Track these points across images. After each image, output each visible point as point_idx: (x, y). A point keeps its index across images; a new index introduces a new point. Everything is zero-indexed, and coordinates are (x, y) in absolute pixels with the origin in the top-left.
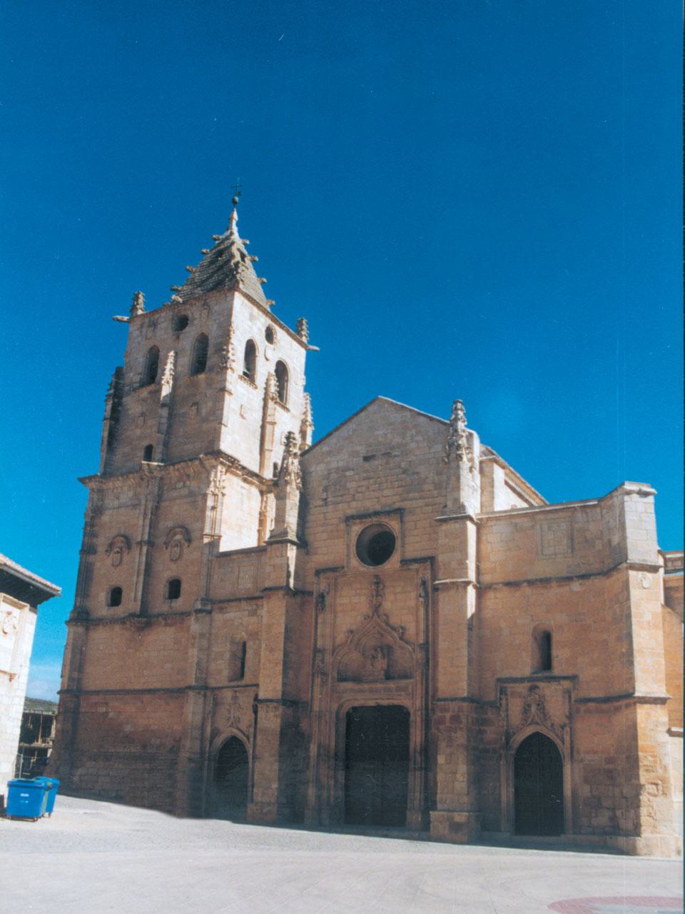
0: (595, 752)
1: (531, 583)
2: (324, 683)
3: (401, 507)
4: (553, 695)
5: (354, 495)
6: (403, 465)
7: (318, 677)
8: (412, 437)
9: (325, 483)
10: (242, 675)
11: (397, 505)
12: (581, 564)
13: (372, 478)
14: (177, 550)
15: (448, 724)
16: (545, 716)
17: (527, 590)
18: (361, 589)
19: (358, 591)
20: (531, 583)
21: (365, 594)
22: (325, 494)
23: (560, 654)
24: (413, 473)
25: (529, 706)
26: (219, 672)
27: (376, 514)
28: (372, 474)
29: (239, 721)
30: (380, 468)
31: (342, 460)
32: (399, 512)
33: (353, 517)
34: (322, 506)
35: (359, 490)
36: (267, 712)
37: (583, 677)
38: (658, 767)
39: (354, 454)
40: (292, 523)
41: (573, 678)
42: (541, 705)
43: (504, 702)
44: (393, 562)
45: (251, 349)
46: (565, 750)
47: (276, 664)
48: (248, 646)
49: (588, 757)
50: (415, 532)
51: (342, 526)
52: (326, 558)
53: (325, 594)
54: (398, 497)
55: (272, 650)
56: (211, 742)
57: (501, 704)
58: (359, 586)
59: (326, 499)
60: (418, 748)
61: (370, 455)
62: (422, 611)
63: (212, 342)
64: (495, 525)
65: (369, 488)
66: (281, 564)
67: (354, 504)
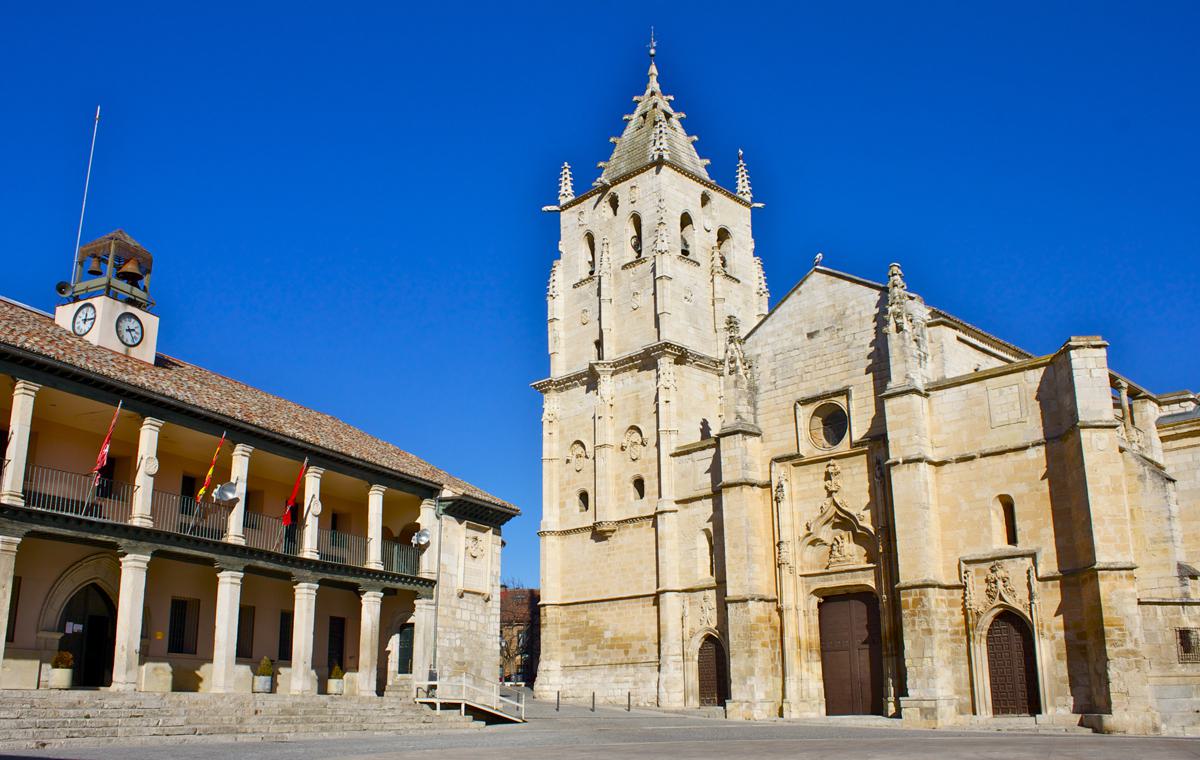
1: (984, 456)
5: (802, 376)
9: (772, 365)
11: (844, 384)
13: (819, 356)
18: (818, 474)
25: (995, 582)
27: (826, 396)
32: (845, 392)
33: (805, 402)
38: (1128, 639)
39: (799, 332)
41: (1033, 556)
52: (781, 444)
53: (783, 483)
54: (845, 374)
58: (816, 471)
60: (888, 635)
61: (813, 331)
67: (803, 385)
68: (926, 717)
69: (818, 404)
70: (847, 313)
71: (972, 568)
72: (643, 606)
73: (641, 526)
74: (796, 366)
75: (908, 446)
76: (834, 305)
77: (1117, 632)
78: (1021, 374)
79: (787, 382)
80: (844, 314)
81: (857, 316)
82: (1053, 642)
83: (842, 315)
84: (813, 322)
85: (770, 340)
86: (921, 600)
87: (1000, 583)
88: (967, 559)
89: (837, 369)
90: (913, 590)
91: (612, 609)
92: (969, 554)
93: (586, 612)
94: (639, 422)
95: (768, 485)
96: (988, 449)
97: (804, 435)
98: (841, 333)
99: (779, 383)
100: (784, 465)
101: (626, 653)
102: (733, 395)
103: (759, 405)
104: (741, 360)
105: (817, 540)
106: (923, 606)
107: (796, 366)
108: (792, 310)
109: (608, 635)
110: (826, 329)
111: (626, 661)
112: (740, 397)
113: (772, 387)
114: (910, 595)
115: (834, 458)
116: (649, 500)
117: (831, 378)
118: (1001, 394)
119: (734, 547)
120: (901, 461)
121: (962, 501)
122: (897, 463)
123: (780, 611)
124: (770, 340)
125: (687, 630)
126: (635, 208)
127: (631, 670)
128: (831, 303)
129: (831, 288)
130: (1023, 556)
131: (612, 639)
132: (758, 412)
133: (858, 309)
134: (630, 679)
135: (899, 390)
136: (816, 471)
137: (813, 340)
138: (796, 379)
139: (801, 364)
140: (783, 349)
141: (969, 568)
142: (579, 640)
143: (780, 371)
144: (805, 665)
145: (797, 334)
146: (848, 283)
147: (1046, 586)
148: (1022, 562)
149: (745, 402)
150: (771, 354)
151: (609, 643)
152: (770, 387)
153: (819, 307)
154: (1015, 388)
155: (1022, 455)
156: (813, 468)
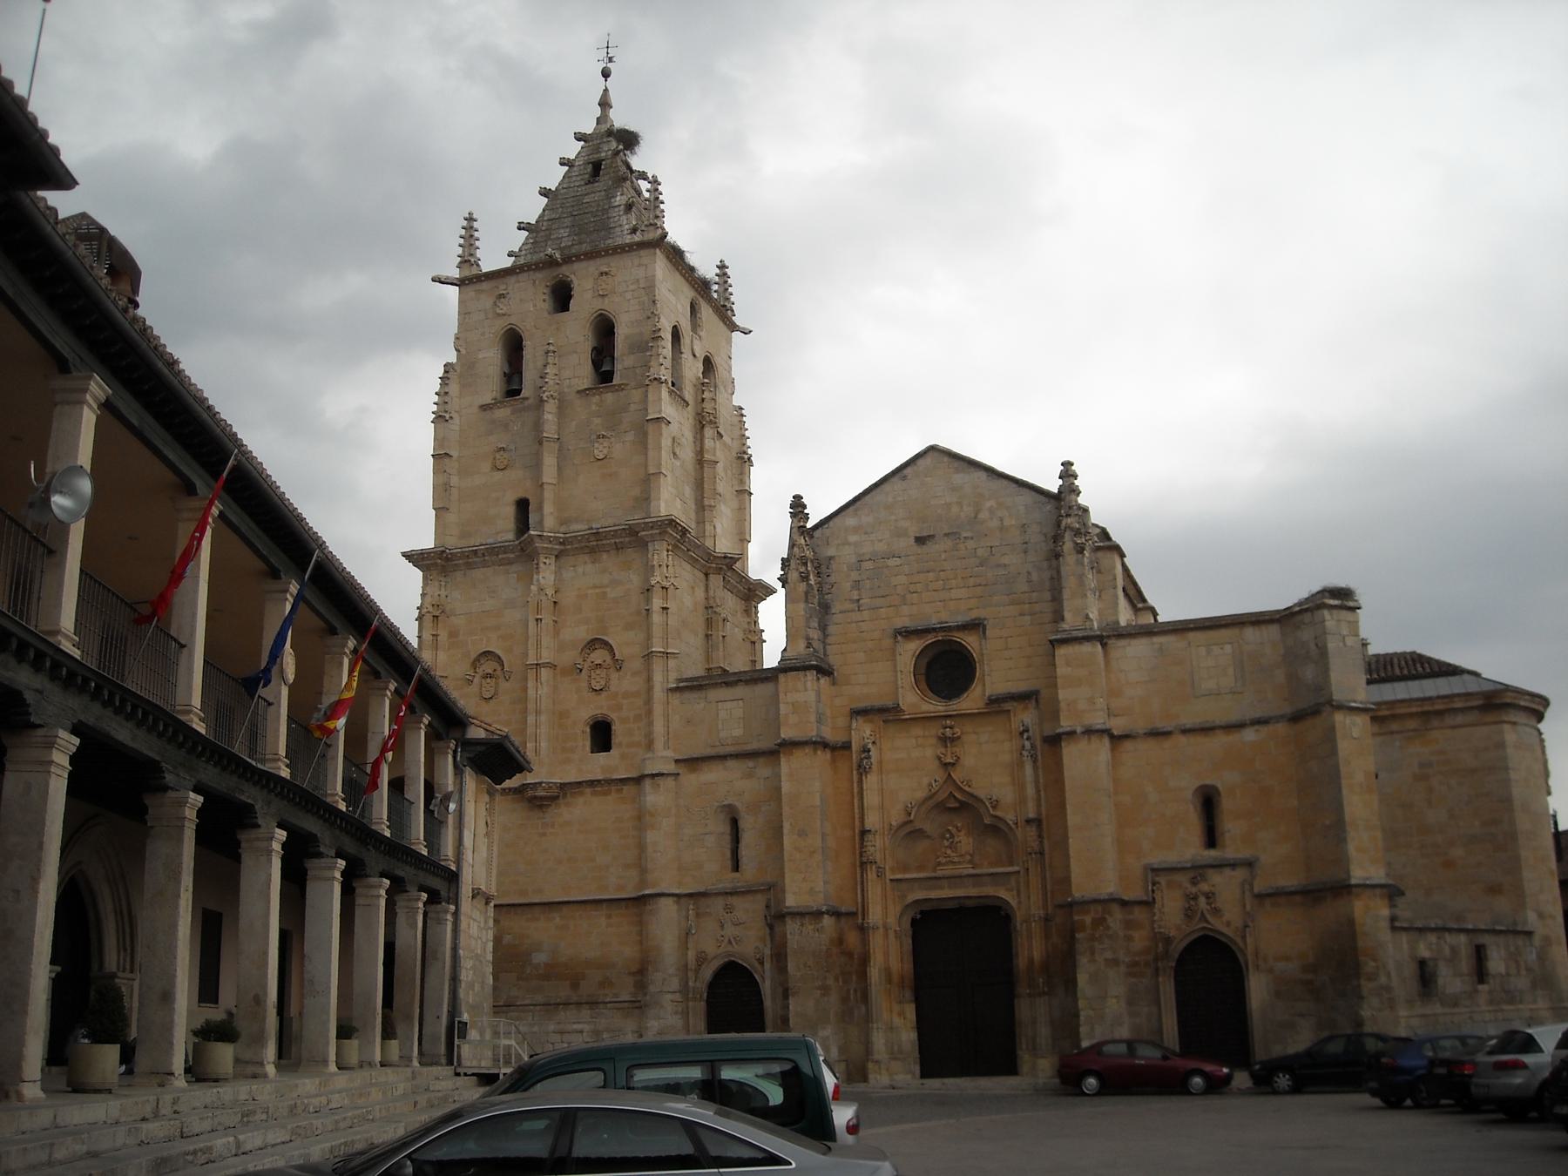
1: (1186, 731)
2: (880, 874)
4: (1226, 886)
5: (904, 596)
6: (980, 552)
7: (871, 868)
8: (991, 510)
9: (854, 575)
10: (736, 867)
11: (974, 614)
13: (933, 571)
16: (1216, 911)
17: (1183, 739)
18: (924, 737)
20: (1186, 731)
22: (856, 592)
23: (1231, 827)
24: (998, 566)
25: (1195, 898)
31: (881, 541)
32: (976, 626)
33: (908, 633)
34: (853, 611)
36: (802, 925)
39: (899, 533)
41: (1249, 864)
42: (1209, 896)
43: (1158, 896)
44: (971, 701)
45: (676, 335)
47: (814, 852)
48: (742, 824)
51: (888, 642)
53: (870, 746)
55: (802, 834)
56: (697, 971)
57: (1154, 899)
59: (858, 600)
61: (925, 534)
63: (622, 332)
64: (1129, 645)
66: (806, 702)
67: (905, 610)
69: (930, 639)
70: (981, 516)
71: (1162, 880)
72: (609, 917)
73: (606, 794)
74: (895, 581)
76: (960, 504)
77: (1373, 964)
79: (879, 602)
80: (976, 517)
81: (995, 523)
85: (853, 538)
86: (1104, 919)
87: (1202, 900)
88: (1155, 866)
92: (1158, 858)
94: (606, 634)
95: (847, 746)
96: (1188, 721)
97: (906, 678)
101: (575, 986)
103: (832, 629)
104: (812, 561)
105: (920, 831)
106: (1108, 928)
109: (540, 958)
110: (946, 535)
111: (575, 999)
112: (811, 617)
113: (854, 606)
115: (950, 716)
116: (623, 757)
119: (800, 835)
120: (1079, 730)
122: (1072, 733)
123: (863, 929)
124: (853, 538)
125: (691, 955)
126: (608, 306)
127: (586, 1013)
130: (1233, 865)
131: (546, 965)
132: (828, 641)
134: (586, 1027)
135: (1080, 634)
139: (902, 579)
141: (1157, 879)
143: (868, 584)
144: (896, 1008)
148: (1233, 873)
149: (816, 625)
150: (853, 560)
152: (848, 606)
156: (917, 730)
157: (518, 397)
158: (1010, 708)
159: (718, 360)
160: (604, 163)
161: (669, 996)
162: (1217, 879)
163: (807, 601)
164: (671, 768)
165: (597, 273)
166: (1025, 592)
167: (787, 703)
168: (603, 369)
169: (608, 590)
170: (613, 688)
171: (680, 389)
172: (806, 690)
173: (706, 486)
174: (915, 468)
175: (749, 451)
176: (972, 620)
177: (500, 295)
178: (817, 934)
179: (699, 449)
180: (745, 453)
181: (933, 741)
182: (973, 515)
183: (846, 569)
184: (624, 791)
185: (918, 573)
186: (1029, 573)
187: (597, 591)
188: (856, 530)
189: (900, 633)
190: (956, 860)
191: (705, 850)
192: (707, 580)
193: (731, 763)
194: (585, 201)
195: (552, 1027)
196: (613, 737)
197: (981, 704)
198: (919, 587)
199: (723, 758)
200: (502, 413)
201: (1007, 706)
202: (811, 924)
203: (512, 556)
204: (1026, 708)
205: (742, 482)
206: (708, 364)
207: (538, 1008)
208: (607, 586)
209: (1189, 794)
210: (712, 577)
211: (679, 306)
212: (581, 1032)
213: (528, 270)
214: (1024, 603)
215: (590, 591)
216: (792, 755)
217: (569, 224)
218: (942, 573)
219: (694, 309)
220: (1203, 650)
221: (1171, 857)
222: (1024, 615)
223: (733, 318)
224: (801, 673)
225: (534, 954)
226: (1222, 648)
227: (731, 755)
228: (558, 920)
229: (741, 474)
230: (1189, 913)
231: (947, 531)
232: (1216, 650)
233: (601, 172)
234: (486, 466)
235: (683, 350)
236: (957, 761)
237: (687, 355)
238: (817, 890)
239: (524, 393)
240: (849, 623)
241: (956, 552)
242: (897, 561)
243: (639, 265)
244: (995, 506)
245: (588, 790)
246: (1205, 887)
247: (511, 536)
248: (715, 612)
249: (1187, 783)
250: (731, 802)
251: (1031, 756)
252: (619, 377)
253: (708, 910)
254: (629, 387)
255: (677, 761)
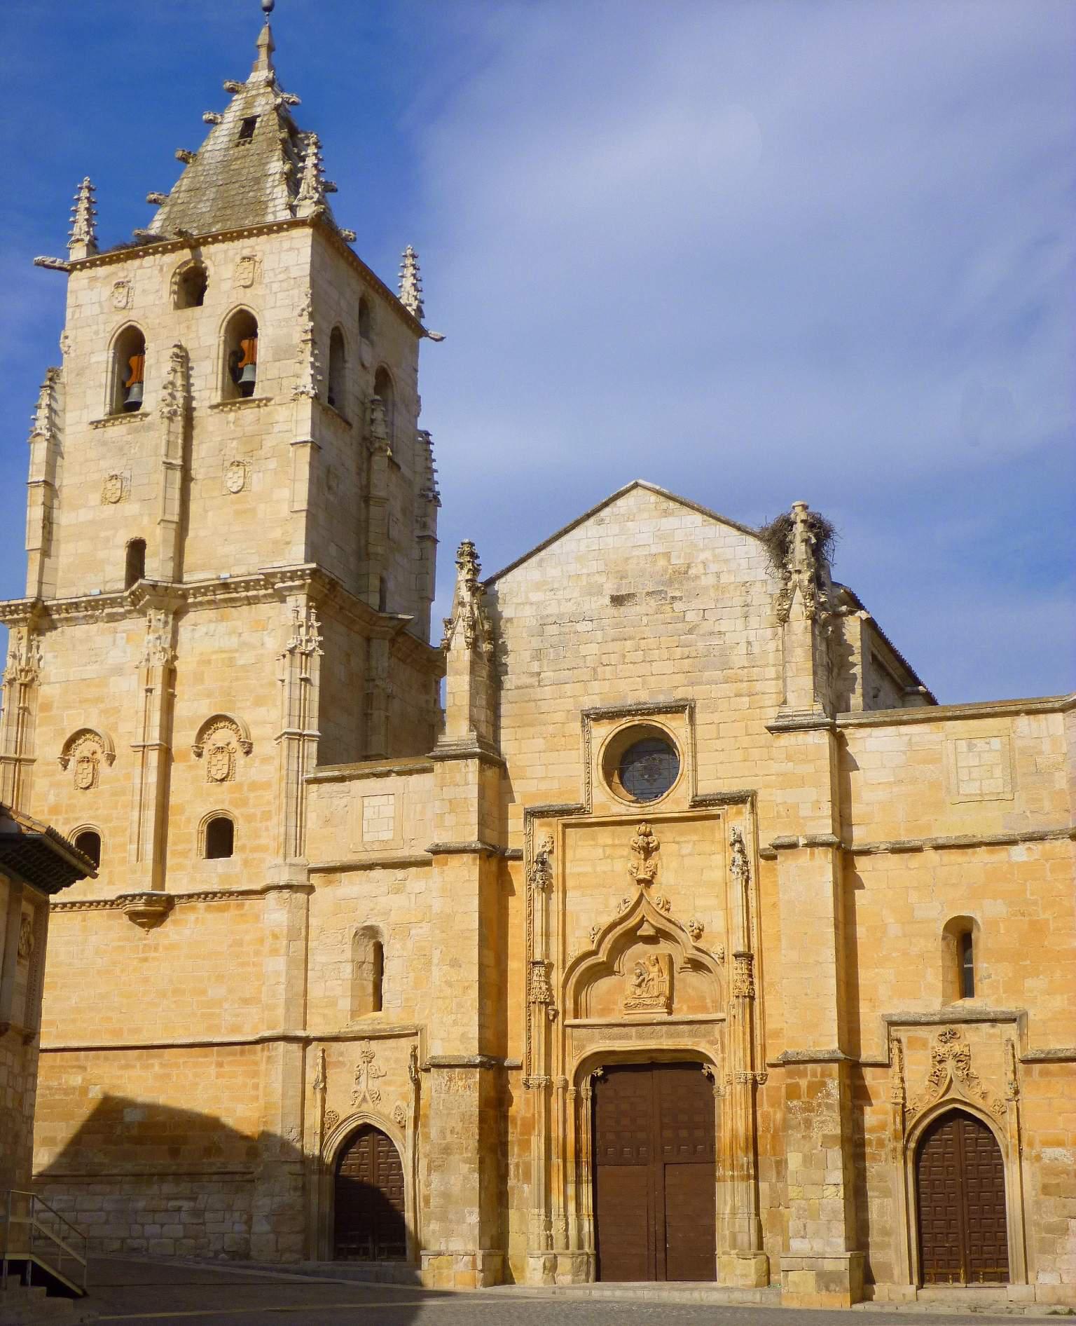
0: (1060, 1144)
1: (938, 848)
3: (690, 697)
9: (536, 643)
11: (680, 694)
12: (1028, 814)
13: (630, 638)
14: (223, 758)
15: (805, 1099)
17: (931, 856)
18: (613, 846)
19: (609, 851)
21: (622, 857)
22: (536, 663)
26: (332, 1003)
28: (629, 631)
29: (379, 1098)
30: (645, 620)
34: (533, 686)
35: (605, 659)
36: (450, 1080)
37: (1034, 1015)
40: (479, 721)
42: (962, 1059)
44: (676, 800)
46: (1005, 1140)
49: (1050, 1153)
50: (718, 744)
51: (577, 725)
52: (543, 786)
59: (539, 674)
61: (623, 593)
62: (738, 889)
64: (870, 736)
65: (624, 656)
67: (596, 686)
68: (827, 1289)
69: (625, 723)
70: (692, 572)
71: (903, 1033)
72: (220, 1065)
73: (221, 910)
74: (584, 650)
75: (813, 818)
76: (667, 555)
78: (1007, 720)
80: (686, 573)
82: (1037, 1165)
83: (682, 574)
84: (621, 579)
86: (824, 1084)
89: (668, 667)
90: (810, 1066)
91: (146, 1067)
93: (84, 1068)
96: (942, 836)
98: (678, 606)
99: (548, 675)
100: (549, 825)
101: (174, 1153)
102: (467, 687)
106: (828, 1095)
107: (584, 650)
108: (583, 548)
110: (648, 594)
113: (534, 681)
114: (803, 1074)
116: (246, 863)
117: (652, 681)
118: (970, 747)
119: (453, 966)
120: (802, 841)
121: (892, 920)
124: (535, 597)
127: (185, 1188)
128: (662, 549)
129: (669, 523)
133: (713, 568)
134: (186, 1205)
135: (804, 720)
136: (609, 841)
137: (622, 608)
138: (584, 674)
139: (593, 649)
140: (561, 616)
142: (63, 1124)
145: (590, 594)
146: (698, 518)
147: (1028, 1073)
148: (992, 1031)
149: (484, 703)
151: (135, 1132)
153: (636, 553)
154: (996, 744)
155: (1001, 855)
156: (605, 836)
157: (137, 413)
158: (719, 812)
159: (396, 372)
160: (259, 120)
161: (287, 1168)
162: (973, 1037)
163: (473, 671)
164: (301, 879)
165: (238, 259)
166: (744, 667)
167: (443, 800)
168: (242, 380)
169: (237, 655)
170: (238, 778)
171: (341, 409)
172: (467, 784)
173: (372, 529)
174: (614, 509)
175: (437, 488)
176: (676, 701)
177: (118, 283)
178: (468, 1093)
179: (364, 482)
180: (431, 490)
181: (626, 851)
182: (683, 569)
183: (525, 635)
184: (246, 907)
185: (613, 641)
186: (749, 643)
187: (224, 655)
188: (538, 586)
189: (588, 716)
190: (648, 1002)
191: (340, 982)
192: (369, 646)
193: (378, 873)
194: (232, 167)
195: (141, 1204)
196: (235, 839)
197: (686, 806)
198: (614, 659)
199: (370, 867)
200: (118, 431)
201: (715, 810)
202: (462, 1079)
203: (121, 610)
204: (739, 813)
205: (424, 526)
206: (383, 379)
207: (127, 1178)
208: (237, 651)
209: (940, 931)
210: (375, 643)
211: (343, 304)
212: (179, 1209)
213: (153, 254)
214: (741, 681)
215: (214, 657)
216: (446, 864)
217: (212, 196)
218: (642, 641)
219: (364, 308)
220: (963, 745)
221: (914, 1009)
222: (740, 695)
223: (423, 322)
224: (461, 762)
225: (126, 1111)
226: (988, 743)
227: (377, 865)
228: (157, 1068)
229: (425, 515)
230: (936, 1078)
231: (650, 591)
232: (980, 744)
233: (256, 132)
234: (95, 498)
235: (347, 358)
236: (652, 877)
237: (351, 364)
238: (471, 1036)
239: (145, 408)
240: (526, 702)
241: (660, 616)
242: (589, 626)
243: (291, 249)
244: (711, 558)
245: (201, 905)
246: (957, 1047)
247: (122, 585)
248: (377, 686)
249: (938, 915)
250: (374, 923)
251: (743, 873)
252: (260, 391)
253: (341, 1059)
254: (273, 402)
255: (312, 871)
